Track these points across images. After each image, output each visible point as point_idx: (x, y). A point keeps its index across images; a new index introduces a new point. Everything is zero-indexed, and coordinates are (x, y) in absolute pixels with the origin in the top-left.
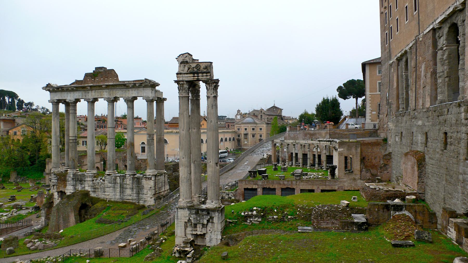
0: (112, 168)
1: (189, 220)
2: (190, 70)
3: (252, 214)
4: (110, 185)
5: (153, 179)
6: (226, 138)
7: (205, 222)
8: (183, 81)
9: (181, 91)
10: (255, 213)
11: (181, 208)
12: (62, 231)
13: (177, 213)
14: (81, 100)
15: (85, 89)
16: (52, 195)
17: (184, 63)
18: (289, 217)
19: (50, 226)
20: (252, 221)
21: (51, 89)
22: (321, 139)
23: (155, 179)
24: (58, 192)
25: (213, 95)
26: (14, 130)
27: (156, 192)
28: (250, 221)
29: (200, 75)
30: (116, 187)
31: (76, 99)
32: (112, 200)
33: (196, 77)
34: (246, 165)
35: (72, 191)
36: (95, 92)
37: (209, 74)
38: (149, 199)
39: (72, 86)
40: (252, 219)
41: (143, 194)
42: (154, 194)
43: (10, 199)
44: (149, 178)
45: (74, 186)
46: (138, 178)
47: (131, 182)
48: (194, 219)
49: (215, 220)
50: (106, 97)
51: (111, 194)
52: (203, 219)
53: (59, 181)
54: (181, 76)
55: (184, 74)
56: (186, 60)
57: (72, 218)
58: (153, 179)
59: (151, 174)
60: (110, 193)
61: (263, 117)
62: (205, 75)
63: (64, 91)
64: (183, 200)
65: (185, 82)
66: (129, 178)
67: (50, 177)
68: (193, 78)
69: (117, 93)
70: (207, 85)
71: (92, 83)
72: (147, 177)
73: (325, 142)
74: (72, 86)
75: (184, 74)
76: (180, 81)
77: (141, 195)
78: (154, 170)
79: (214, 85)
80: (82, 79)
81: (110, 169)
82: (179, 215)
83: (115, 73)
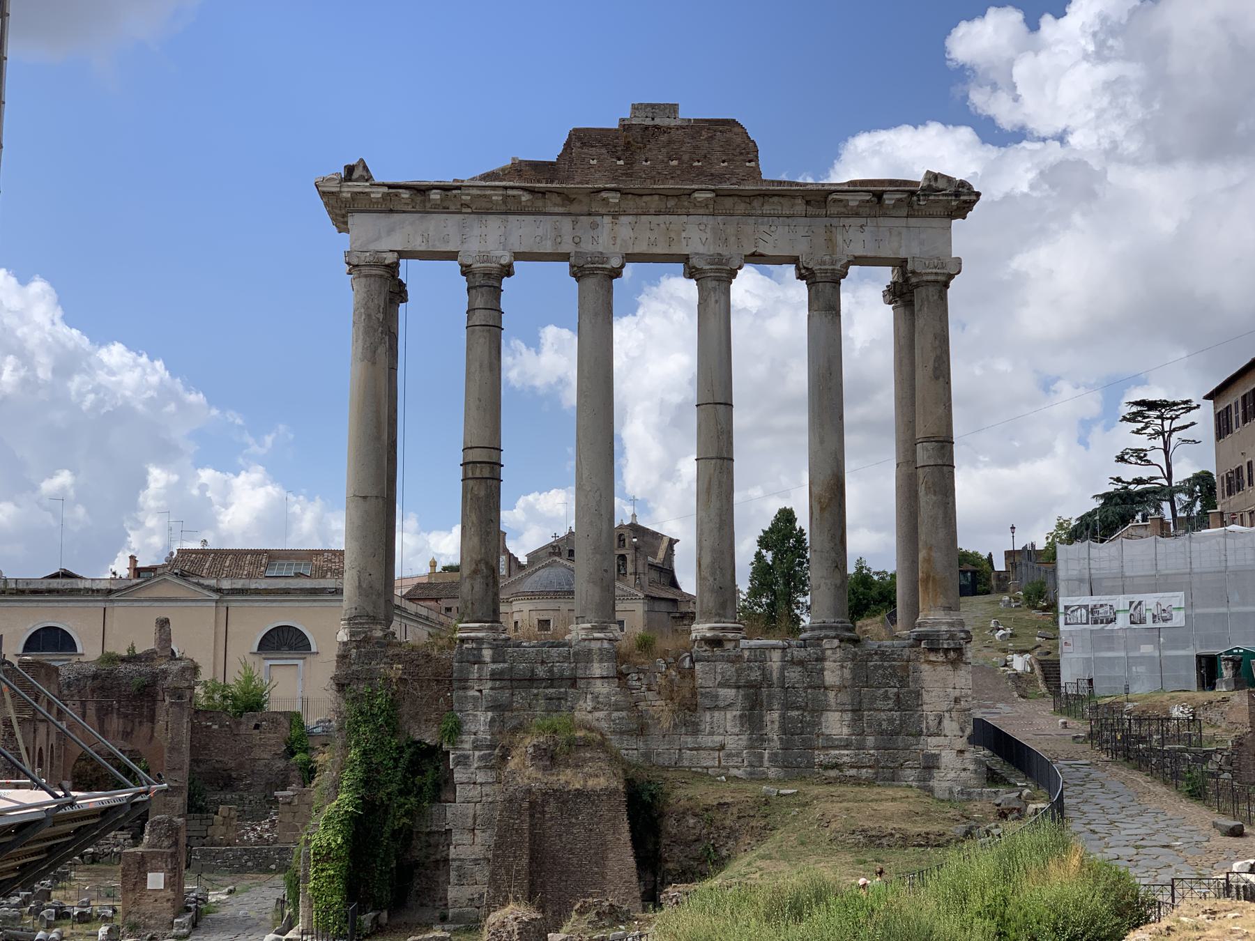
15: (575, 208)
44: (947, 651)
50: (701, 249)
66: (839, 653)
71: (614, 179)
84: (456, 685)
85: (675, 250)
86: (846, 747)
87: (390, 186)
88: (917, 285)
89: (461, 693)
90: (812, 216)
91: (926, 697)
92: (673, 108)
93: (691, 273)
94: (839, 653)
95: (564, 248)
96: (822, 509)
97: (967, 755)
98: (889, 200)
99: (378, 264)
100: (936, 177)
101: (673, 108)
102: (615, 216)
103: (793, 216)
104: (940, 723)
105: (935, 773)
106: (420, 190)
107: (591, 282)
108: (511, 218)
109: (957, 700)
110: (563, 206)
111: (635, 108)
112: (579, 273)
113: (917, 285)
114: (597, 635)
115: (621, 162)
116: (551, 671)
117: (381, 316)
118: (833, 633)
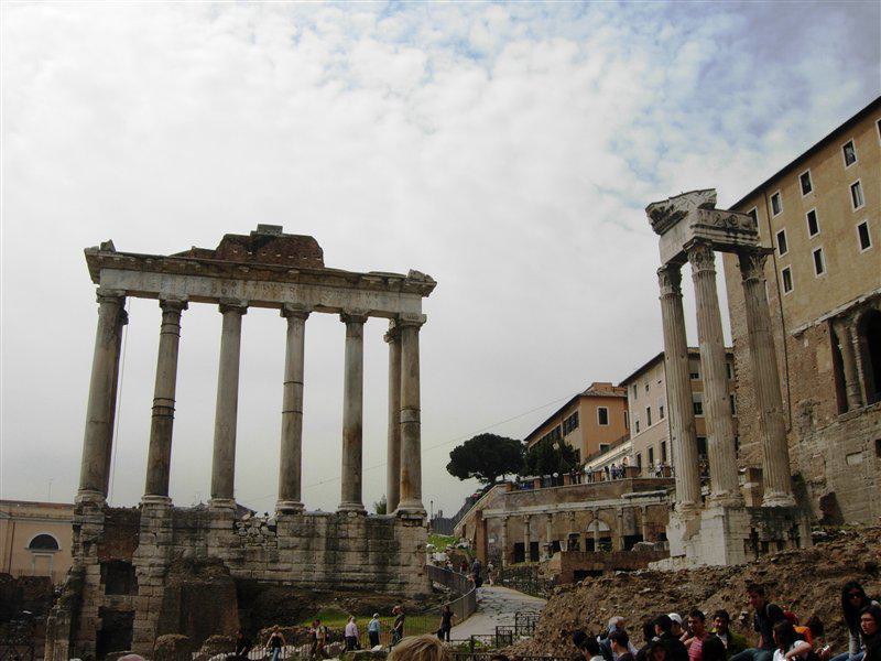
4: (294, 540)
15: (224, 274)
30: (314, 544)
38: (413, 577)
41: (398, 565)
44: (414, 520)
51: (295, 567)
72: (412, 517)
77: (390, 569)
84: (142, 529)
85: (276, 300)
86: (359, 571)
87: (124, 254)
88: (404, 328)
89: (144, 534)
92: (281, 228)
93: (285, 313)
95: (216, 295)
96: (350, 442)
98: (391, 282)
99: (115, 296)
100: (415, 272)
101: (281, 228)
103: (341, 287)
106: (141, 259)
107: (230, 314)
109: (419, 547)
111: (260, 226)
112: (223, 310)
113: (404, 328)
114: (223, 505)
117: (113, 325)
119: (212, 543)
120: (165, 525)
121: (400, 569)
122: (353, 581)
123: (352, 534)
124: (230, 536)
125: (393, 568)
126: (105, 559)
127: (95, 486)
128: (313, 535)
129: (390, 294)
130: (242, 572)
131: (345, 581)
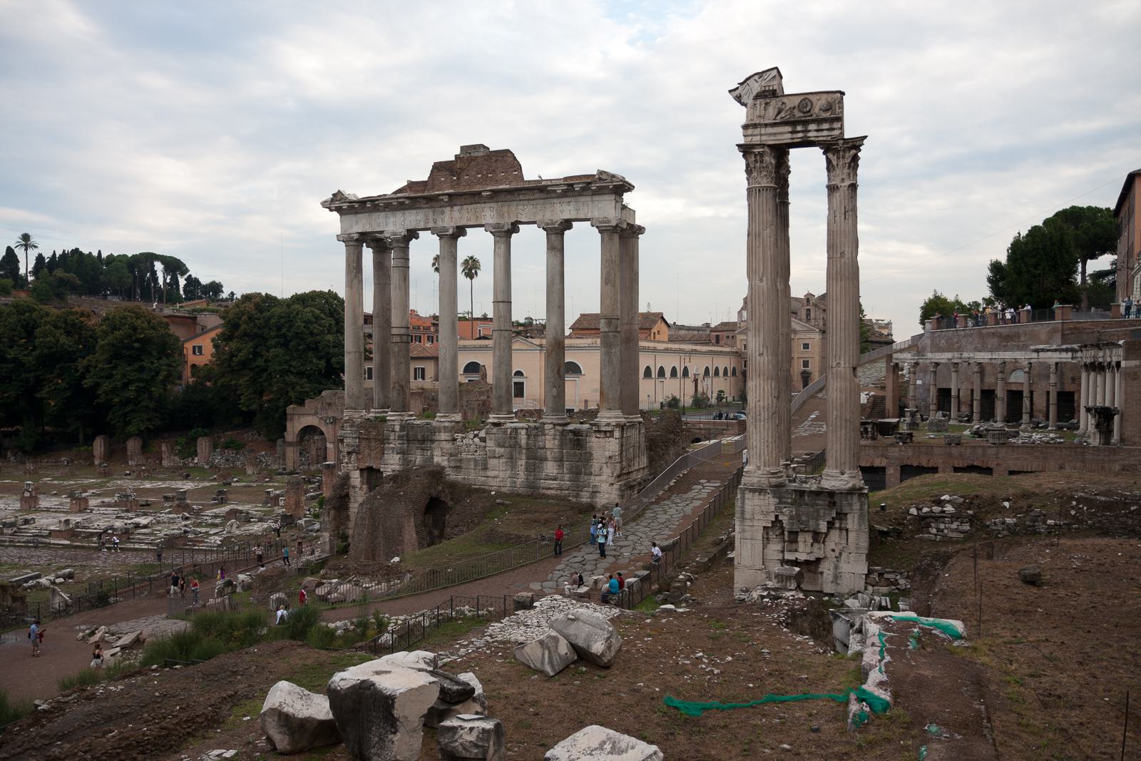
0: (504, 408)
1: (777, 521)
2: (783, 114)
3: (944, 512)
4: (501, 450)
5: (617, 434)
6: (717, 368)
7: (823, 527)
8: (764, 145)
9: (755, 174)
10: (949, 508)
11: (753, 491)
12: (397, 559)
13: (743, 503)
14: (421, 233)
15: (433, 204)
16: (347, 477)
17: (766, 97)
18: (1049, 522)
19: (352, 552)
20: (942, 531)
21: (345, 206)
22: (1041, 347)
23: (622, 437)
24: (361, 470)
25: (847, 183)
26: (196, 342)
27: (622, 469)
28: (938, 530)
29: (812, 127)
30: (516, 455)
31: (408, 231)
32: (503, 490)
33: (800, 135)
34: (813, 420)
35: (397, 468)
36: (460, 211)
37: (837, 125)
39: (399, 195)
40: (942, 526)
41: (591, 474)
42: (619, 476)
43: (214, 499)
44: (605, 432)
45: (402, 452)
46: (576, 433)
47: (557, 442)
48: (791, 518)
49: (852, 522)
50: (491, 221)
52: (817, 518)
53: (364, 443)
54: (757, 131)
55: (766, 125)
56: (763, 91)
57: (410, 534)
58: (617, 434)
59: (613, 422)
60: (500, 476)
61: (812, 315)
62: (826, 126)
63: (378, 210)
64: (759, 468)
65: (767, 149)
66: (552, 432)
67: (340, 433)
68: (789, 136)
69: (522, 210)
70: (830, 155)
71: (452, 188)
73: (1057, 355)
74: (399, 195)
75: (766, 125)
76: (753, 146)
77: (583, 478)
78: (619, 413)
79: (844, 153)
80: (425, 178)
81: (499, 411)
82: (748, 507)
83: (515, 158)
85: (478, 223)
86: (555, 479)
90: (544, 199)
91: (595, 456)
94: (552, 432)
95: (429, 226)
97: (615, 486)
102: (452, 207)
104: (601, 469)
105: (598, 495)
108: (407, 212)
109: (610, 457)
110: (427, 203)
114: (442, 420)
115: (455, 178)
116: (423, 436)
117: (355, 265)
118: (549, 421)
119: (436, 454)
120: (400, 437)
121: (592, 477)
122: (549, 488)
123: (548, 445)
124: (448, 446)
125: (586, 477)
126: (363, 466)
127: (353, 405)
128: (515, 445)
129: (583, 199)
130: (460, 477)
131: (543, 488)
